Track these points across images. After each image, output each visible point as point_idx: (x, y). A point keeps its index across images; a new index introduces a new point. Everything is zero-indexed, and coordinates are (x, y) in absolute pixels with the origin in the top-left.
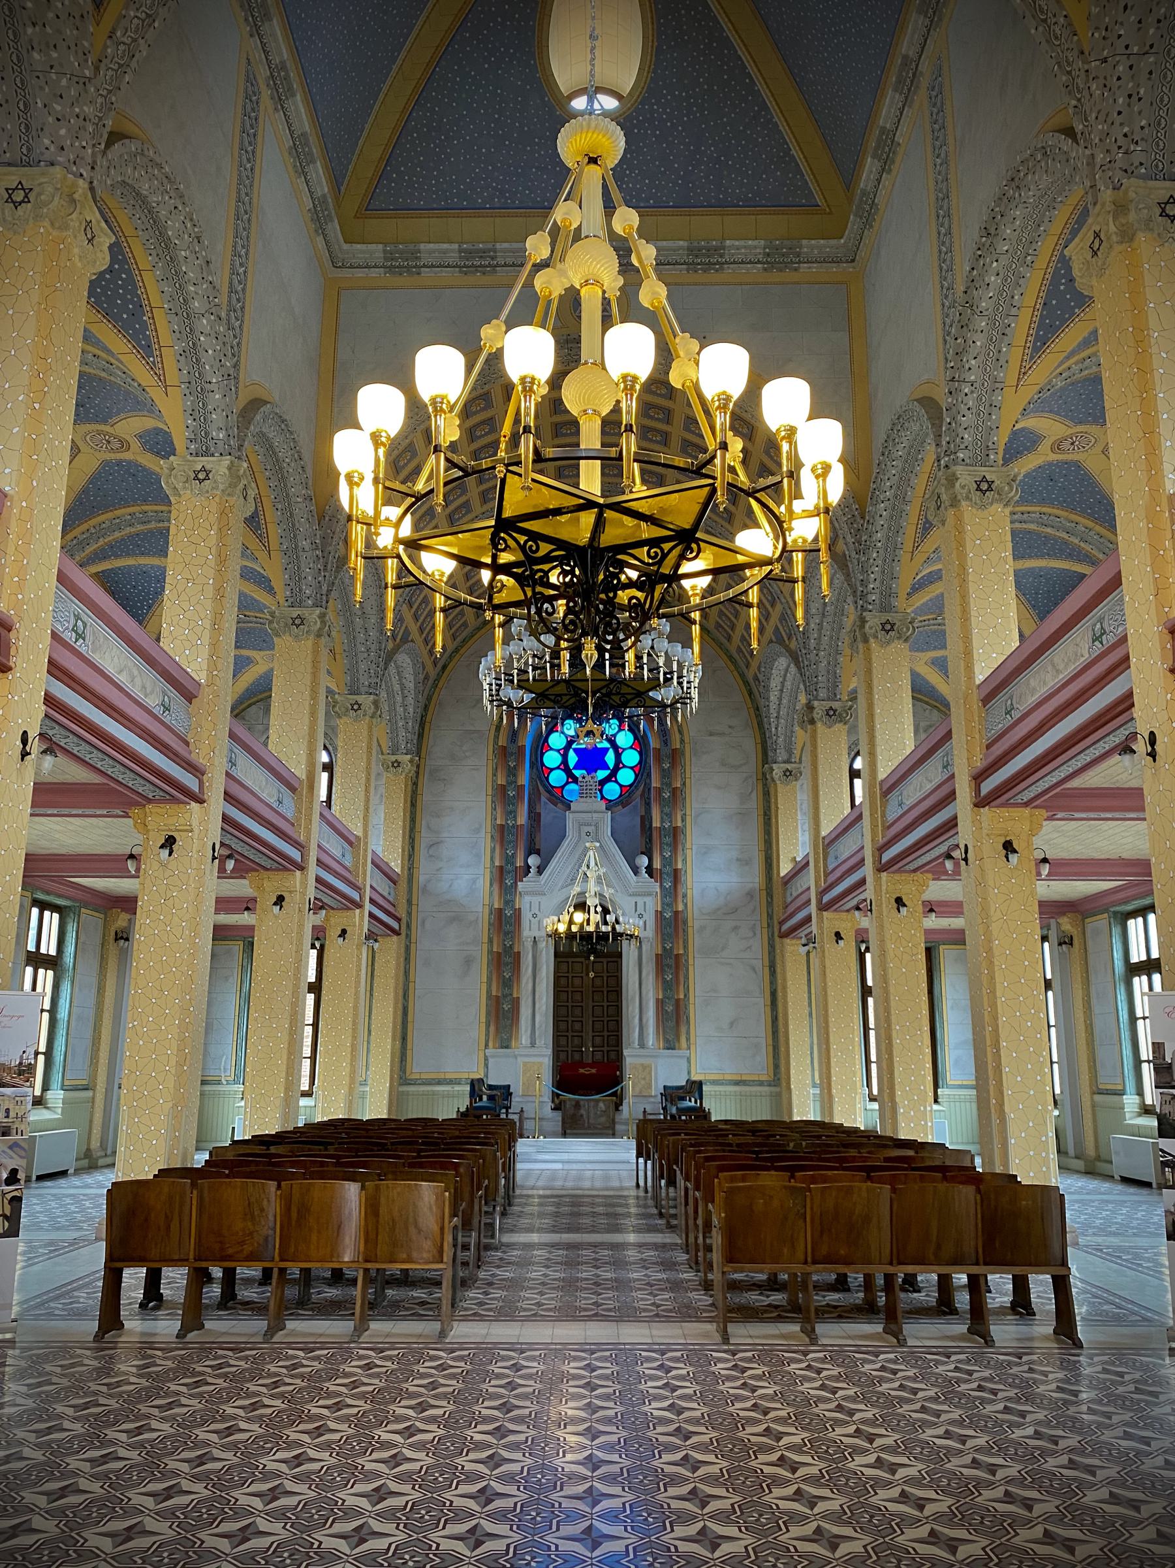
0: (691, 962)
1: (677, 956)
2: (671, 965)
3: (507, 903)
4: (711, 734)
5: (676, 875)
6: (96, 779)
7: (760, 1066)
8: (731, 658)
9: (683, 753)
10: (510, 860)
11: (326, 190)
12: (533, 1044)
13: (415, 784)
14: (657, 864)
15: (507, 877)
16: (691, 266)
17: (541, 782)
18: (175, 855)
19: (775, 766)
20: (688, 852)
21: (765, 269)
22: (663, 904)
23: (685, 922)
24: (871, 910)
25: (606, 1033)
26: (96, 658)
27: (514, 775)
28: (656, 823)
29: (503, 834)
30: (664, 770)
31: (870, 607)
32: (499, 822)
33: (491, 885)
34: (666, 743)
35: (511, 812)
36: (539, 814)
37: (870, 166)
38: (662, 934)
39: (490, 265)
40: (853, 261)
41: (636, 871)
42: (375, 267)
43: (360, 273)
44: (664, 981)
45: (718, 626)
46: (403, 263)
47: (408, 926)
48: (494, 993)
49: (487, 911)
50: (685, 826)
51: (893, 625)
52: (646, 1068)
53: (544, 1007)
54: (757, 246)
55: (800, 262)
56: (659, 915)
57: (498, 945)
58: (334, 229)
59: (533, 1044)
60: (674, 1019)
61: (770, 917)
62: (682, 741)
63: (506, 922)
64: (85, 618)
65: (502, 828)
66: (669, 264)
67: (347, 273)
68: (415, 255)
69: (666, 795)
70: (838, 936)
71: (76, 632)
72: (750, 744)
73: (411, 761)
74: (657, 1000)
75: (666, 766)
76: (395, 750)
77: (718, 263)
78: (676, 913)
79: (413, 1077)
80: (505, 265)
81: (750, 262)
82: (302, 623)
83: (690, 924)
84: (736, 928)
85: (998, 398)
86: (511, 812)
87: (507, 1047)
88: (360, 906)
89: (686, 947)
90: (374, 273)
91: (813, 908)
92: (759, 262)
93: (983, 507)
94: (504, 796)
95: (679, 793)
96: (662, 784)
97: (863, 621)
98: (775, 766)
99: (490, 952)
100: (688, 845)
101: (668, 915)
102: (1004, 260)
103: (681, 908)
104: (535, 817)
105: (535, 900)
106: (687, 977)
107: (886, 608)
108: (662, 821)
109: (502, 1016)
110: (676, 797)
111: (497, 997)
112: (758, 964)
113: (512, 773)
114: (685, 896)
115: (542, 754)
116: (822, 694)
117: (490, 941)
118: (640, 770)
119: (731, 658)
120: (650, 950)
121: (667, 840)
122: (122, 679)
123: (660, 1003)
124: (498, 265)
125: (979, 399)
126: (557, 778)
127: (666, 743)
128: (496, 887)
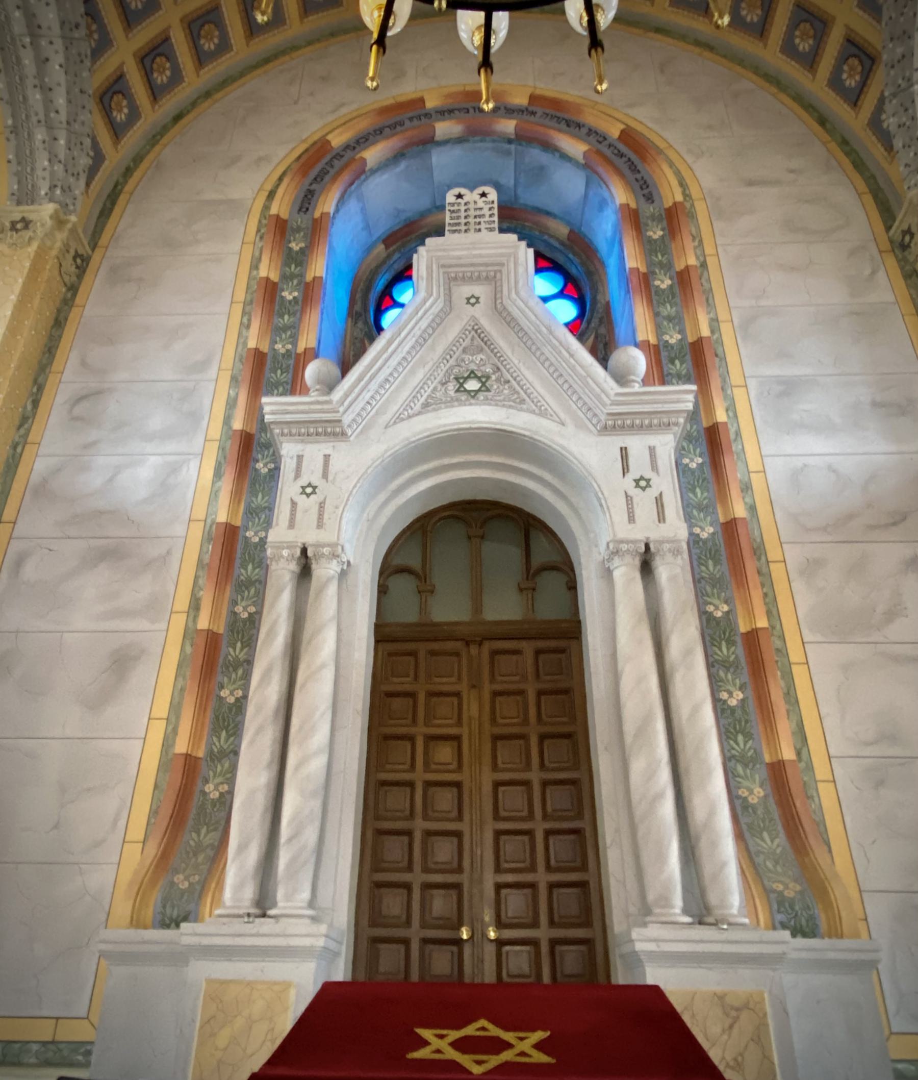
0: (795, 654)
1: (752, 639)
3: (251, 512)
9: (692, 216)
12: (263, 905)
20: (739, 394)
23: (759, 551)
25: (542, 878)
30: (650, 241)
33: (218, 475)
35: (285, 329)
53: (318, 764)
57: (215, 615)
59: (263, 905)
69: (664, 283)
75: (656, 233)
78: (730, 528)
83: (773, 553)
86: (285, 329)
89: (772, 612)
96: (650, 264)
99: (189, 633)
100: (735, 377)
103: (740, 511)
105: (314, 452)
106: (791, 696)
113: (296, 261)
114: (747, 488)
127: (649, 198)
128: (226, 485)
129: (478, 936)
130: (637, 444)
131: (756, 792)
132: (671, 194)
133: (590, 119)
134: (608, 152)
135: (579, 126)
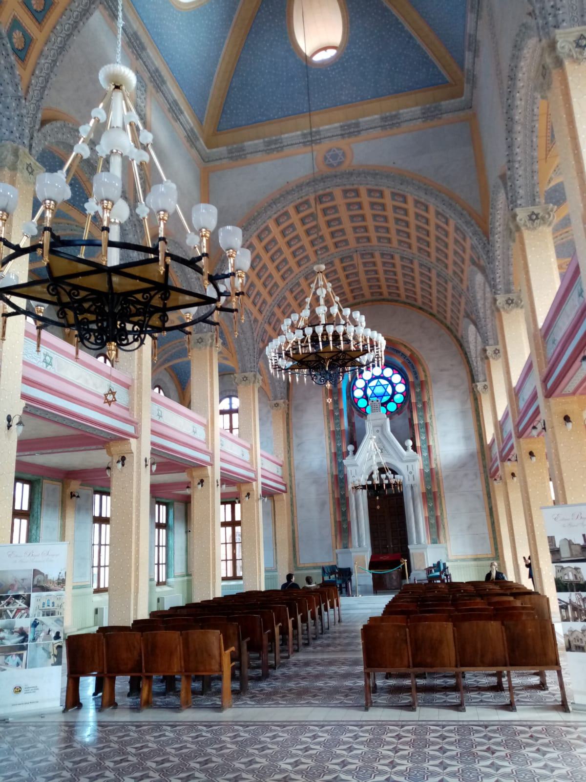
0: (442, 495)
1: (434, 493)
2: (432, 497)
4: (442, 370)
5: (429, 448)
6: (79, 433)
7: (487, 549)
8: (448, 328)
10: (339, 448)
11: (192, 125)
13: (288, 414)
14: (418, 444)
15: (338, 457)
16: (383, 127)
17: (354, 406)
18: (125, 465)
19: (478, 384)
20: (435, 436)
21: (424, 121)
22: (423, 465)
23: (437, 473)
24: (516, 460)
26: (62, 374)
27: (337, 404)
28: (416, 421)
29: (335, 435)
31: (499, 292)
32: (331, 429)
33: (331, 462)
34: (417, 378)
36: (354, 423)
37: (468, 56)
38: (425, 482)
39: (280, 147)
40: (471, 107)
41: (405, 448)
42: (224, 158)
43: (218, 163)
44: (429, 507)
45: (438, 312)
46: (238, 155)
47: (291, 488)
48: (338, 520)
49: (330, 476)
50: (432, 422)
51: (512, 301)
52: (422, 555)
54: (417, 110)
55: (441, 114)
56: (422, 472)
58: (201, 142)
60: (436, 527)
61: (485, 467)
62: (426, 376)
63: (340, 480)
64: (51, 355)
65: (334, 432)
66: (371, 128)
67: (211, 164)
68: (242, 149)
70: (513, 475)
71: (46, 362)
72: (464, 374)
73: (284, 402)
74: (426, 517)
76: (275, 398)
77: (397, 123)
78: (431, 469)
79: (303, 566)
80: (288, 145)
81: (415, 119)
82: (202, 341)
84: (466, 475)
85: (536, 167)
87: (347, 548)
88: (256, 480)
89: (439, 487)
90: (225, 161)
91: (498, 462)
92: (419, 118)
93: (534, 229)
94: (334, 414)
95: (426, 404)
97: (495, 300)
98: (478, 384)
99: (333, 498)
100: (435, 432)
101: (427, 470)
102: (523, 91)
104: (351, 423)
106: (441, 504)
107: (508, 291)
108: (419, 420)
109: (343, 530)
110: (424, 407)
111: (340, 522)
112: (481, 493)
114: (436, 460)
115: (353, 391)
116: (491, 342)
117: (333, 492)
118: (407, 394)
119: (448, 328)
120: (419, 489)
121: (423, 430)
122: (80, 382)
123: (427, 519)
124: (284, 146)
125: (525, 170)
126: (362, 403)
127: (417, 378)
128: (333, 463)
129: (390, 546)
130: (410, 464)
131: (433, 521)
132: (422, 377)
133: (403, 349)
134: (407, 361)
135: (399, 352)
